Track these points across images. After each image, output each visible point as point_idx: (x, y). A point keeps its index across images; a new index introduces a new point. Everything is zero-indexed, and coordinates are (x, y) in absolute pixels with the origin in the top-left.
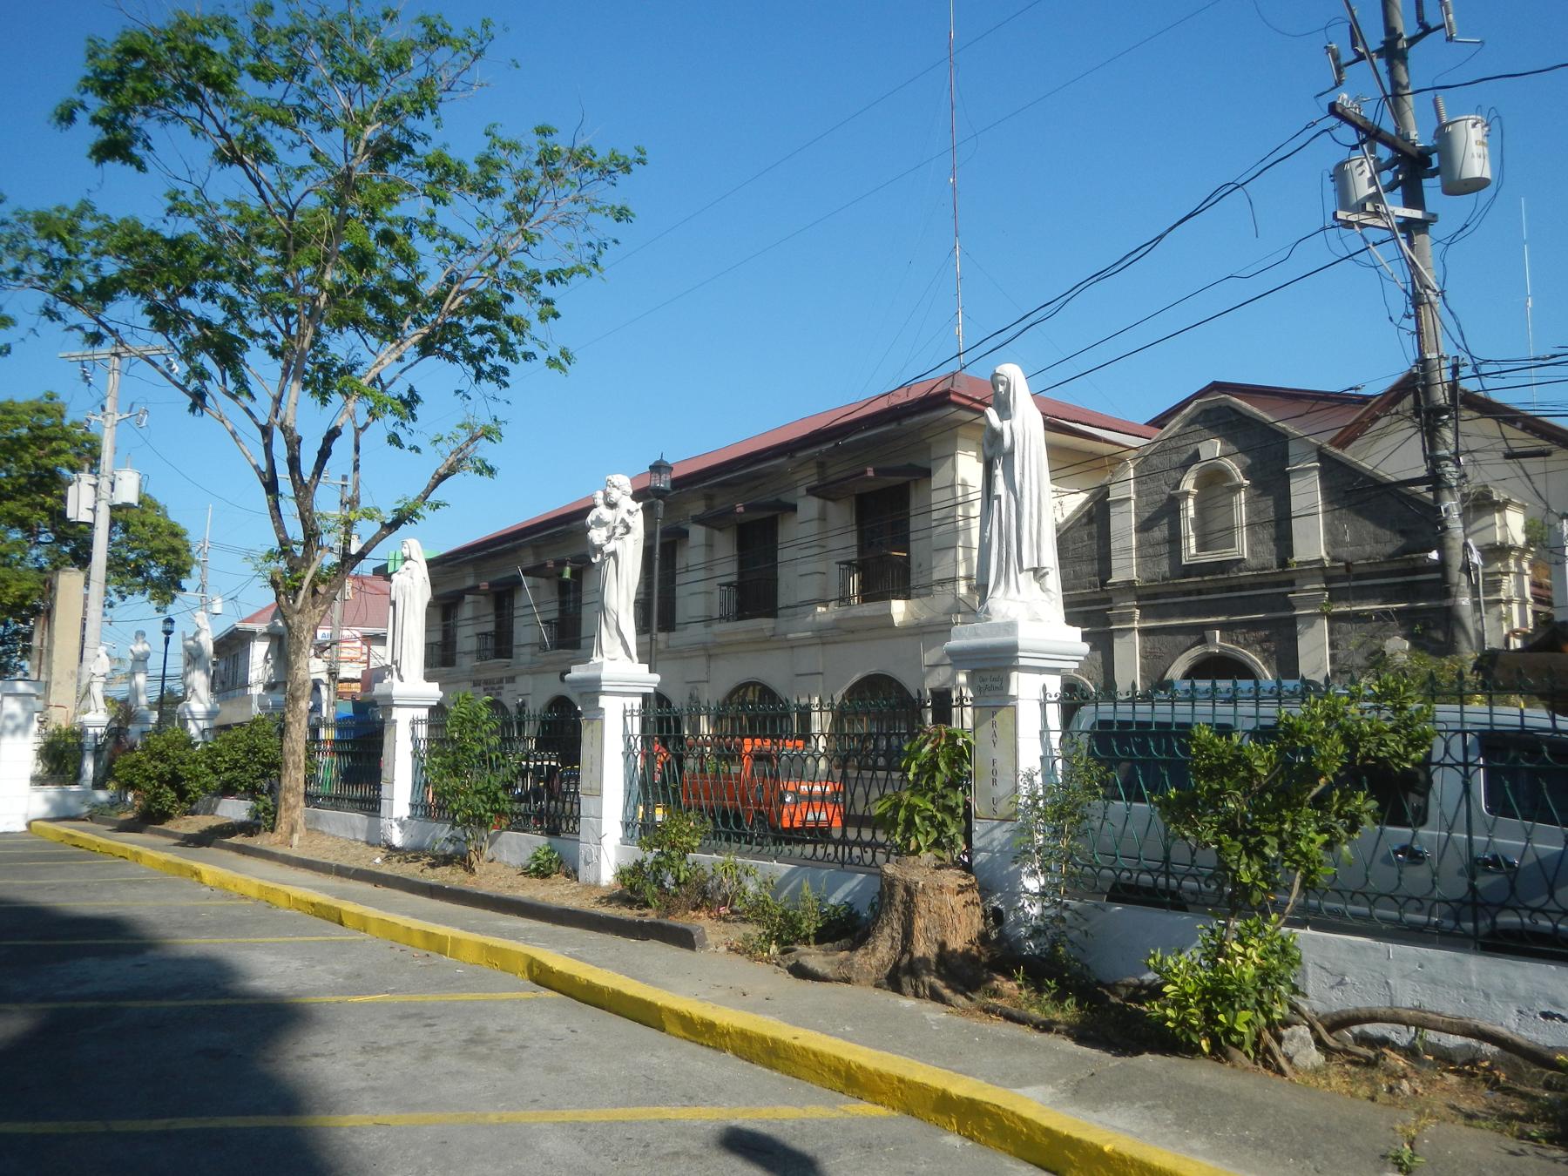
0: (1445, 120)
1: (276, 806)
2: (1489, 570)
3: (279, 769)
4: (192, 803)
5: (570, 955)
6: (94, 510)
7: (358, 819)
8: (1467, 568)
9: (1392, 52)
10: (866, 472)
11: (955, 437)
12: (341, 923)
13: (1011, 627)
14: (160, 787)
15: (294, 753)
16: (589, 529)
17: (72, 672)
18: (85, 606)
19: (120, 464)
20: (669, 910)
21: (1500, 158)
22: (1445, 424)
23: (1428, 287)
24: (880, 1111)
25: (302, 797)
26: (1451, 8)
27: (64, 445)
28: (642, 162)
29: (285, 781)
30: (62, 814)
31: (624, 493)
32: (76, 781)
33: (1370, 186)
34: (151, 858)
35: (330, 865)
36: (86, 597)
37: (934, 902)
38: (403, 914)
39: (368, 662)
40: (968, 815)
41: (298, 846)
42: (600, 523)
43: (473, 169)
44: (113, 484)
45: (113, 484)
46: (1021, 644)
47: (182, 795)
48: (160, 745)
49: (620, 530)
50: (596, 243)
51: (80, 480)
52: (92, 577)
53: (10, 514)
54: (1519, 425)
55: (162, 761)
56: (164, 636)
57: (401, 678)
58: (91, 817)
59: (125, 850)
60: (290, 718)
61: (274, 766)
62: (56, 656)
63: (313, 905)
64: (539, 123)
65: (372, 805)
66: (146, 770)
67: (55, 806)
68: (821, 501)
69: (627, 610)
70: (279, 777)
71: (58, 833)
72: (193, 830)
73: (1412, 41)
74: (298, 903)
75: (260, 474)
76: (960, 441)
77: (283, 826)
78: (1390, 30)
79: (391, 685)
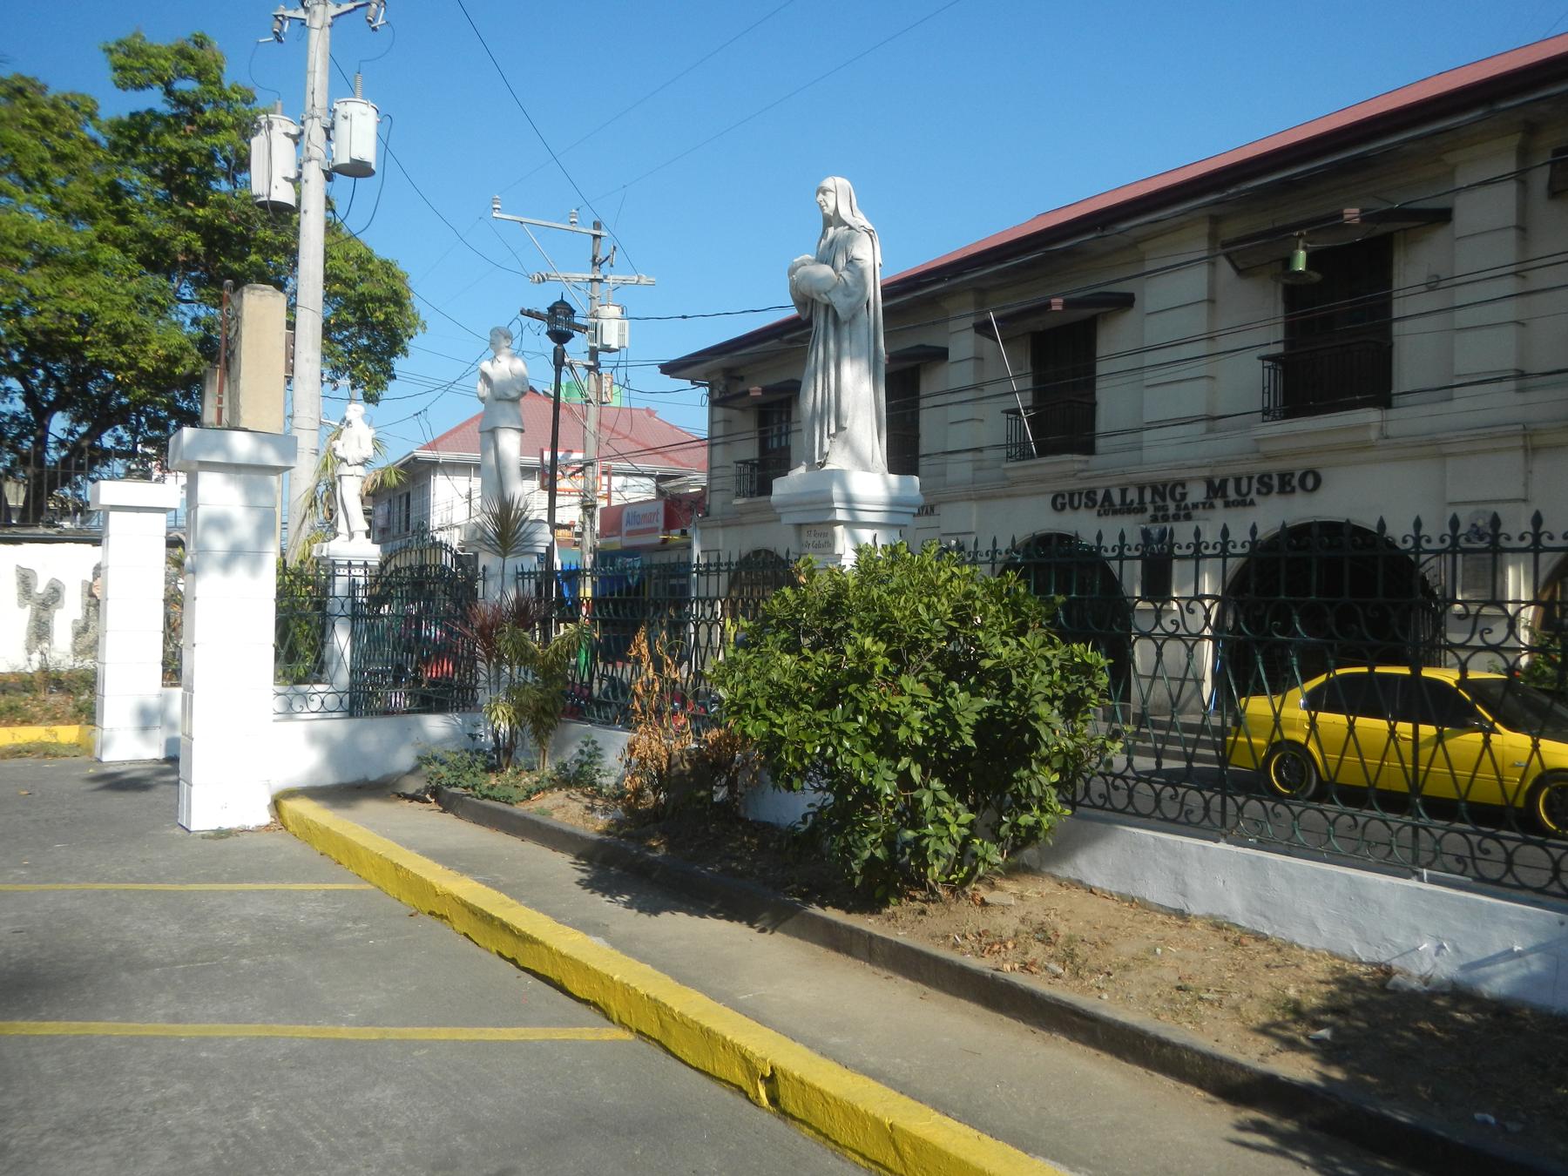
6: (297, 181)
18: (291, 355)
19: (342, 84)
30: (351, 777)
32: (318, 671)
36: (291, 342)
39: (609, 497)
44: (328, 131)
45: (328, 131)
51: (270, 125)
52: (301, 300)
53: (145, 236)
56: (551, 345)
58: (441, 797)
67: (336, 753)
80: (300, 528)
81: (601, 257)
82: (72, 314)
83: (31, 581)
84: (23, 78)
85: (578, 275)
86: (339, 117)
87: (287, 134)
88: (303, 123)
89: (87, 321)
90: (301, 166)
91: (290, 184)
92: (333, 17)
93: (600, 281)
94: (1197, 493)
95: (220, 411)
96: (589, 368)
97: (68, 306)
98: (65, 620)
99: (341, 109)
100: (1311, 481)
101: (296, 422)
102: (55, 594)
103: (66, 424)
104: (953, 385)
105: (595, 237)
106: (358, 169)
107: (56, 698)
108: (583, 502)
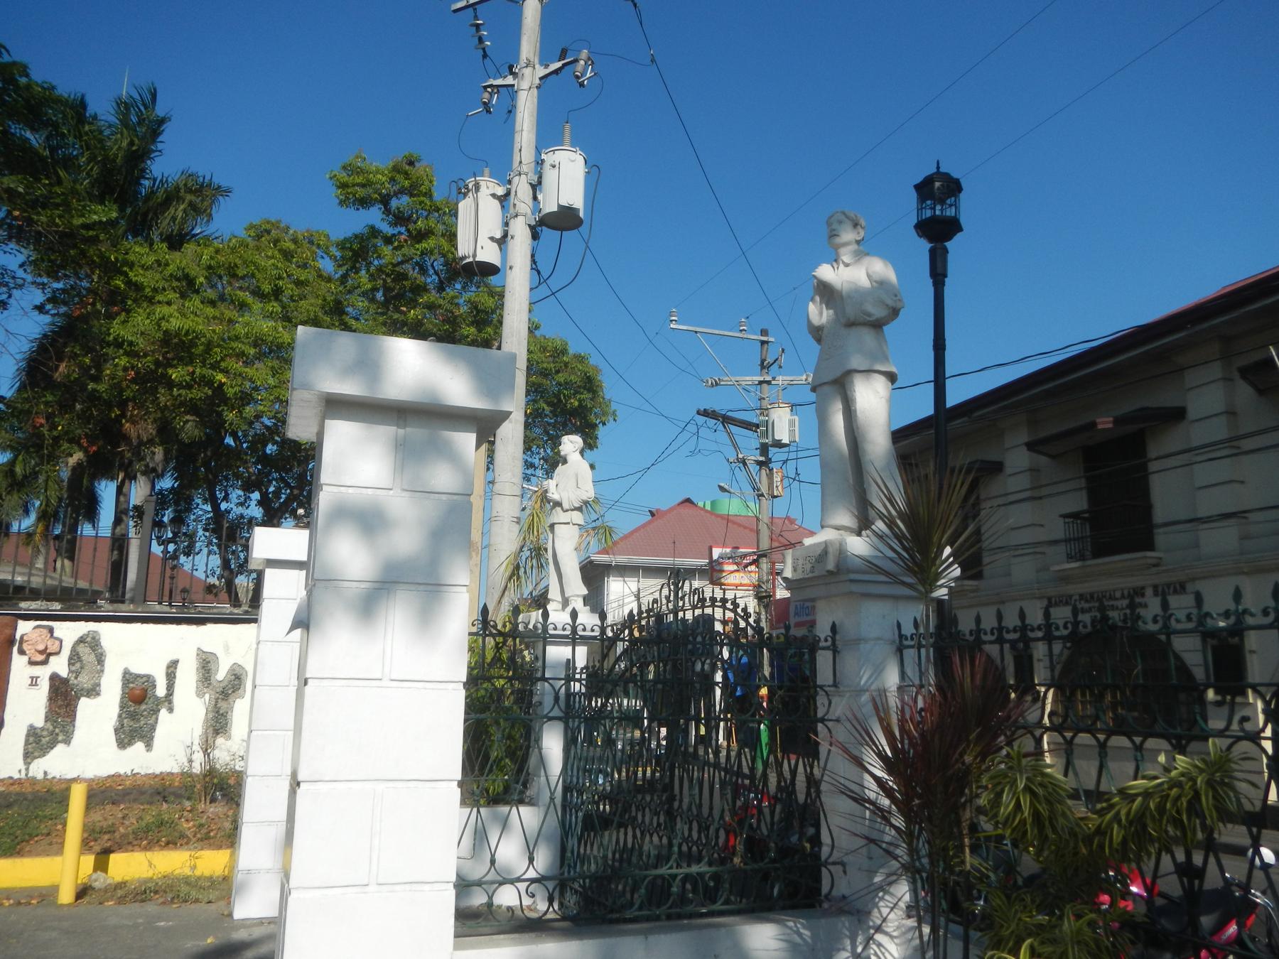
19: (547, 138)
44: (536, 187)
45: (536, 187)
56: (924, 246)
80: (500, 602)
81: (769, 360)
83: (212, 666)
85: (748, 378)
86: (547, 166)
87: (494, 196)
88: (510, 182)
90: (507, 224)
91: (495, 245)
92: (541, 79)
93: (769, 383)
96: (760, 464)
99: (548, 158)
101: (497, 487)
102: (236, 681)
104: (1195, 444)
105: (763, 343)
106: (565, 220)
108: (758, 593)
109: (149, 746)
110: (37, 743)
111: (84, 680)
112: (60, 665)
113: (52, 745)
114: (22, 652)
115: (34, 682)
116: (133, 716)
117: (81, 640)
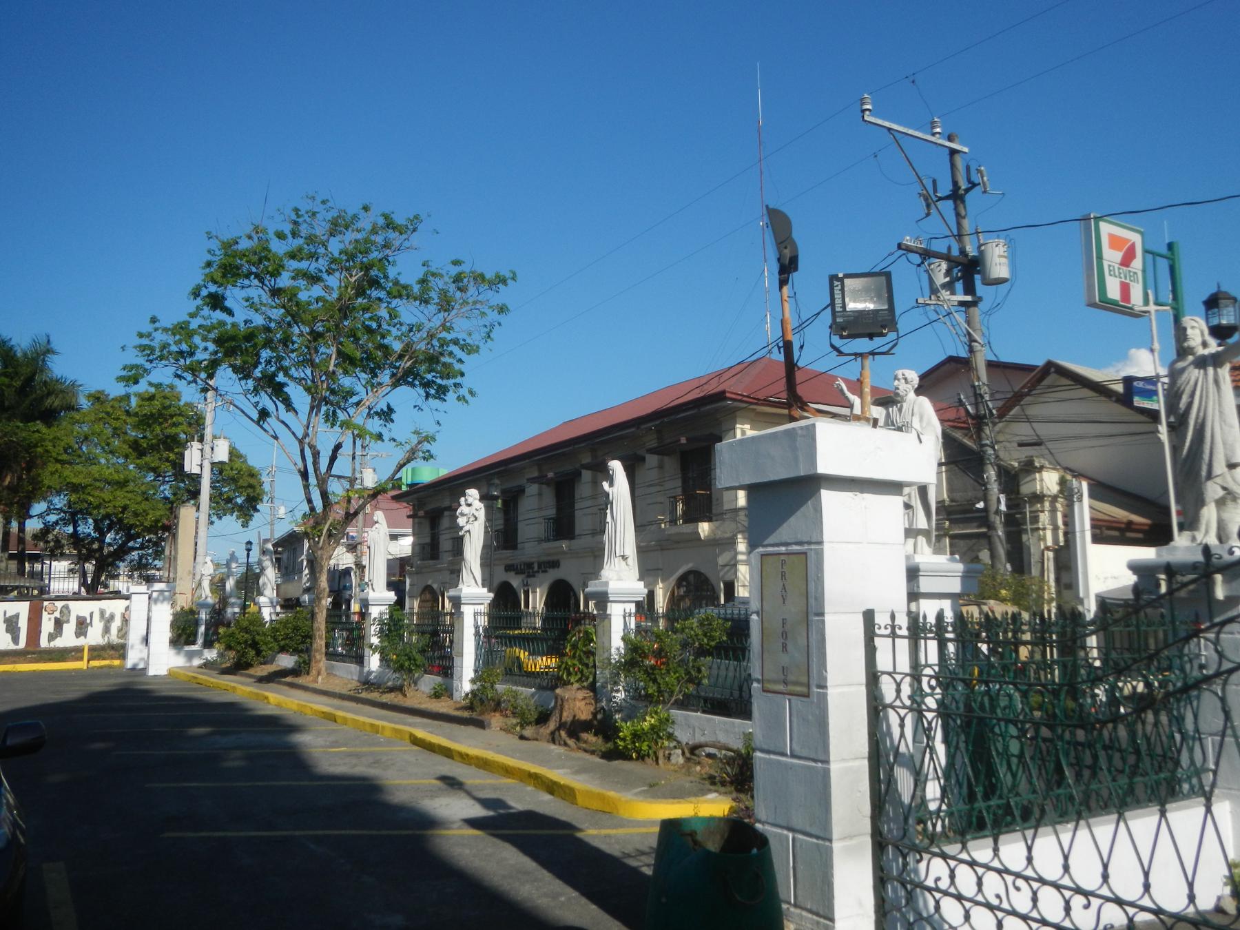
0: (982, 242)
1: (310, 660)
2: (1034, 509)
3: (311, 639)
4: (264, 657)
5: (428, 732)
6: (201, 466)
7: (354, 667)
8: (998, 512)
9: (956, 196)
10: (680, 440)
11: (736, 417)
12: (336, 721)
13: (606, 584)
14: (246, 648)
15: (319, 630)
16: (458, 517)
17: (189, 571)
18: (197, 528)
20: (482, 713)
21: (1013, 266)
22: (987, 425)
23: (976, 341)
24: (513, 781)
25: (323, 656)
26: (985, 173)
27: (181, 419)
28: (513, 279)
29: (315, 646)
31: (475, 499)
32: (194, 643)
33: (945, 277)
34: (242, 690)
35: (336, 693)
37: (572, 705)
38: (363, 716)
40: (594, 666)
41: (321, 682)
42: (462, 514)
43: (416, 289)
45: (212, 449)
46: (609, 592)
47: (258, 653)
48: (245, 624)
49: (472, 519)
50: (488, 324)
54: (1114, 399)
55: (247, 633)
57: (373, 590)
59: (227, 685)
60: (316, 610)
61: (308, 637)
62: (179, 562)
63: (323, 713)
64: (454, 258)
65: (360, 660)
66: (237, 639)
68: (660, 457)
69: (475, 561)
70: (311, 642)
71: (188, 676)
72: (265, 673)
73: (967, 190)
74: (316, 712)
75: (299, 471)
76: (738, 420)
77: (314, 672)
78: (955, 183)
79: (368, 593)
82: (119, 506)
84: (99, 392)
89: (125, 508)
94: (536, 568)
95: (171, 552)
97: (117, 504)
98: (116, 625)
100: (555, 564)
102: (112, 617)
103: (113, 536)
107: (112, 652)
109: (85, 637)
110: (52, 637)
111: (65, 619)
112: (57, 614)
113: (56, 637)
114: (46, 610)
115: (50, 619)
116: (81, 629)
117: (63, 606)
